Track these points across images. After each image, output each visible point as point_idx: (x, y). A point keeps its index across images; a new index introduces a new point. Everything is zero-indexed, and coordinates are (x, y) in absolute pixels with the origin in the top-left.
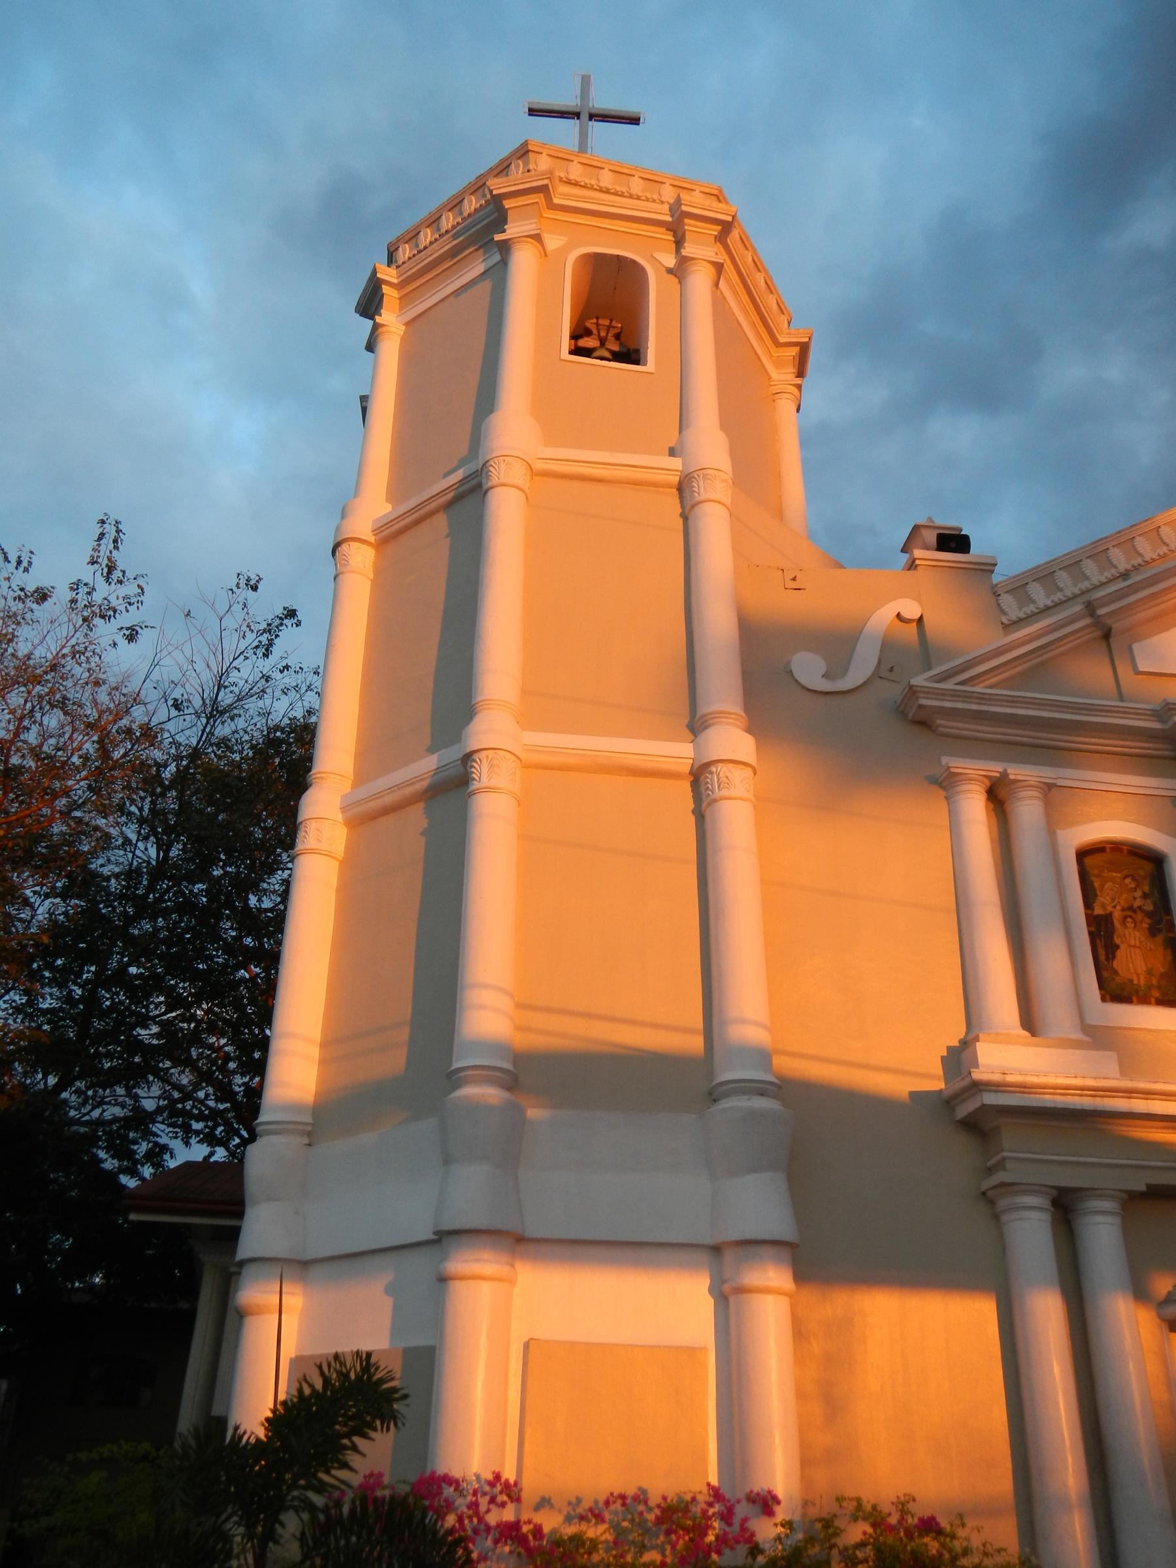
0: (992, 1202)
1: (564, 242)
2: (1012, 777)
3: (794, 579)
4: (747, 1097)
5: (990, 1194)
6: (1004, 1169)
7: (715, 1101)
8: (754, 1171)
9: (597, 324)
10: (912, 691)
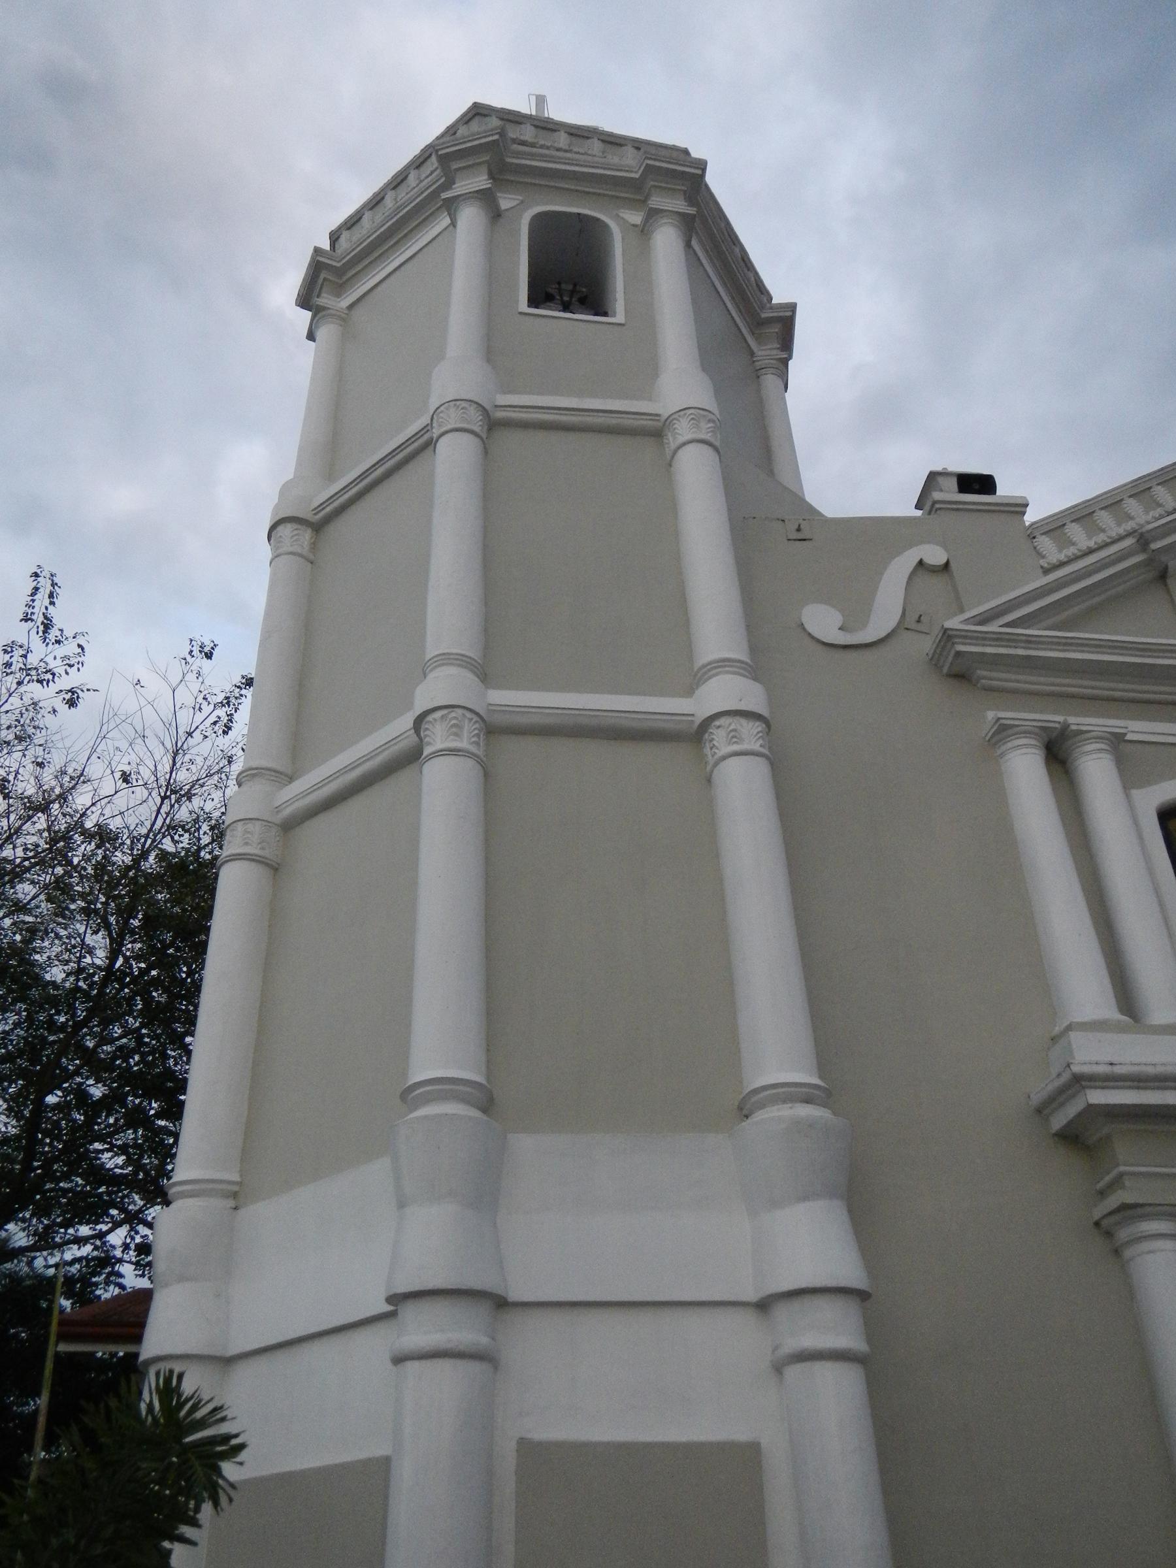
0: (1109, 1234)
1: (518, 202)
2: (1074, 727)
3: (799, 530)
4: (790, 1105)
5: (1105, 1223)
6: (1123, 1187)
7: (747, 1117)
8: (805, 1198)
9: (560, 290)
10: (948, 636)
